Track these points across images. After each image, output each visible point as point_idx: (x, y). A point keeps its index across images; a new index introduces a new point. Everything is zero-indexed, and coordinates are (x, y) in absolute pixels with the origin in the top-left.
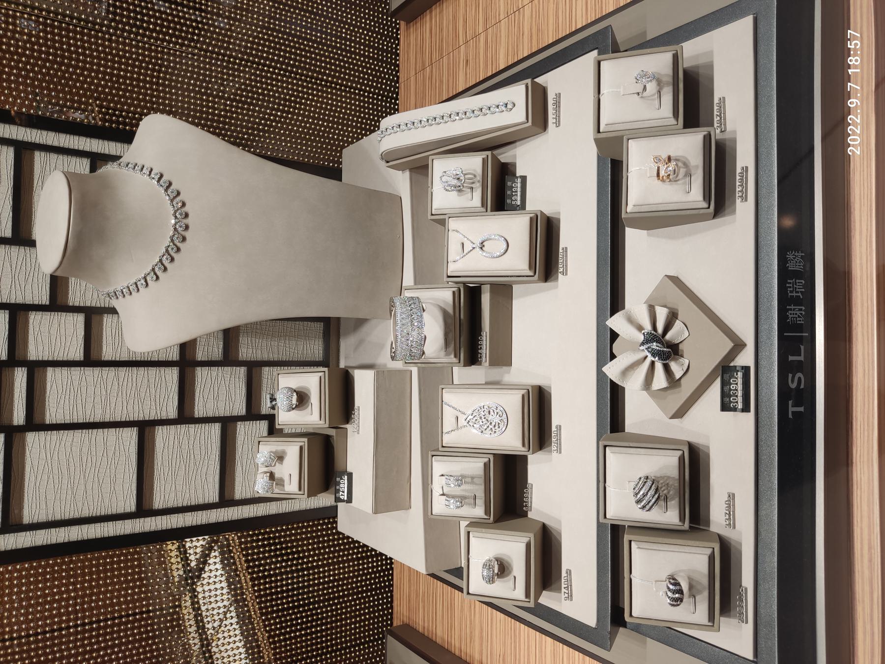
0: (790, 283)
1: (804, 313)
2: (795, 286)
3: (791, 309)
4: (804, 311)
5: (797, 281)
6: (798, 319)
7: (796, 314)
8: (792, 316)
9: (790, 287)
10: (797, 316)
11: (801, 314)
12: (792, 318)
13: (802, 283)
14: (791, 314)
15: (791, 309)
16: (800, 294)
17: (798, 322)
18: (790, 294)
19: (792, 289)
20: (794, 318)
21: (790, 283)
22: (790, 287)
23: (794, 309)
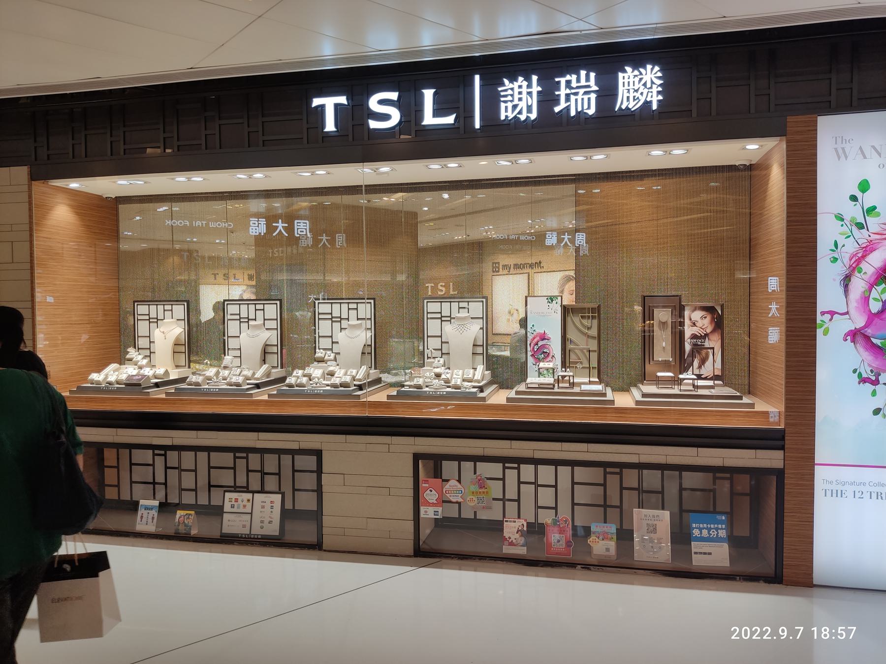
0: (588, 79)
1: (523, 117)
2: (582, 91)
3: (529, 86)
4: (528, 117)
5: (593, 96)
6: (510, 105)
7: (520, 99)
8: (517, 90)
9: (578, 80)
10: (516, 102)
11: (520, 113)
12: (512, 89)
13: (589, 108)
14: (520, 87)
15: (529, 86)
16: (563, 105)
17: (503, 105)
18: (563, 80)
19: (574, 84)
20: (512, 95)
21: (588, 79)
22: (578, 80)
23: (530, 93)
